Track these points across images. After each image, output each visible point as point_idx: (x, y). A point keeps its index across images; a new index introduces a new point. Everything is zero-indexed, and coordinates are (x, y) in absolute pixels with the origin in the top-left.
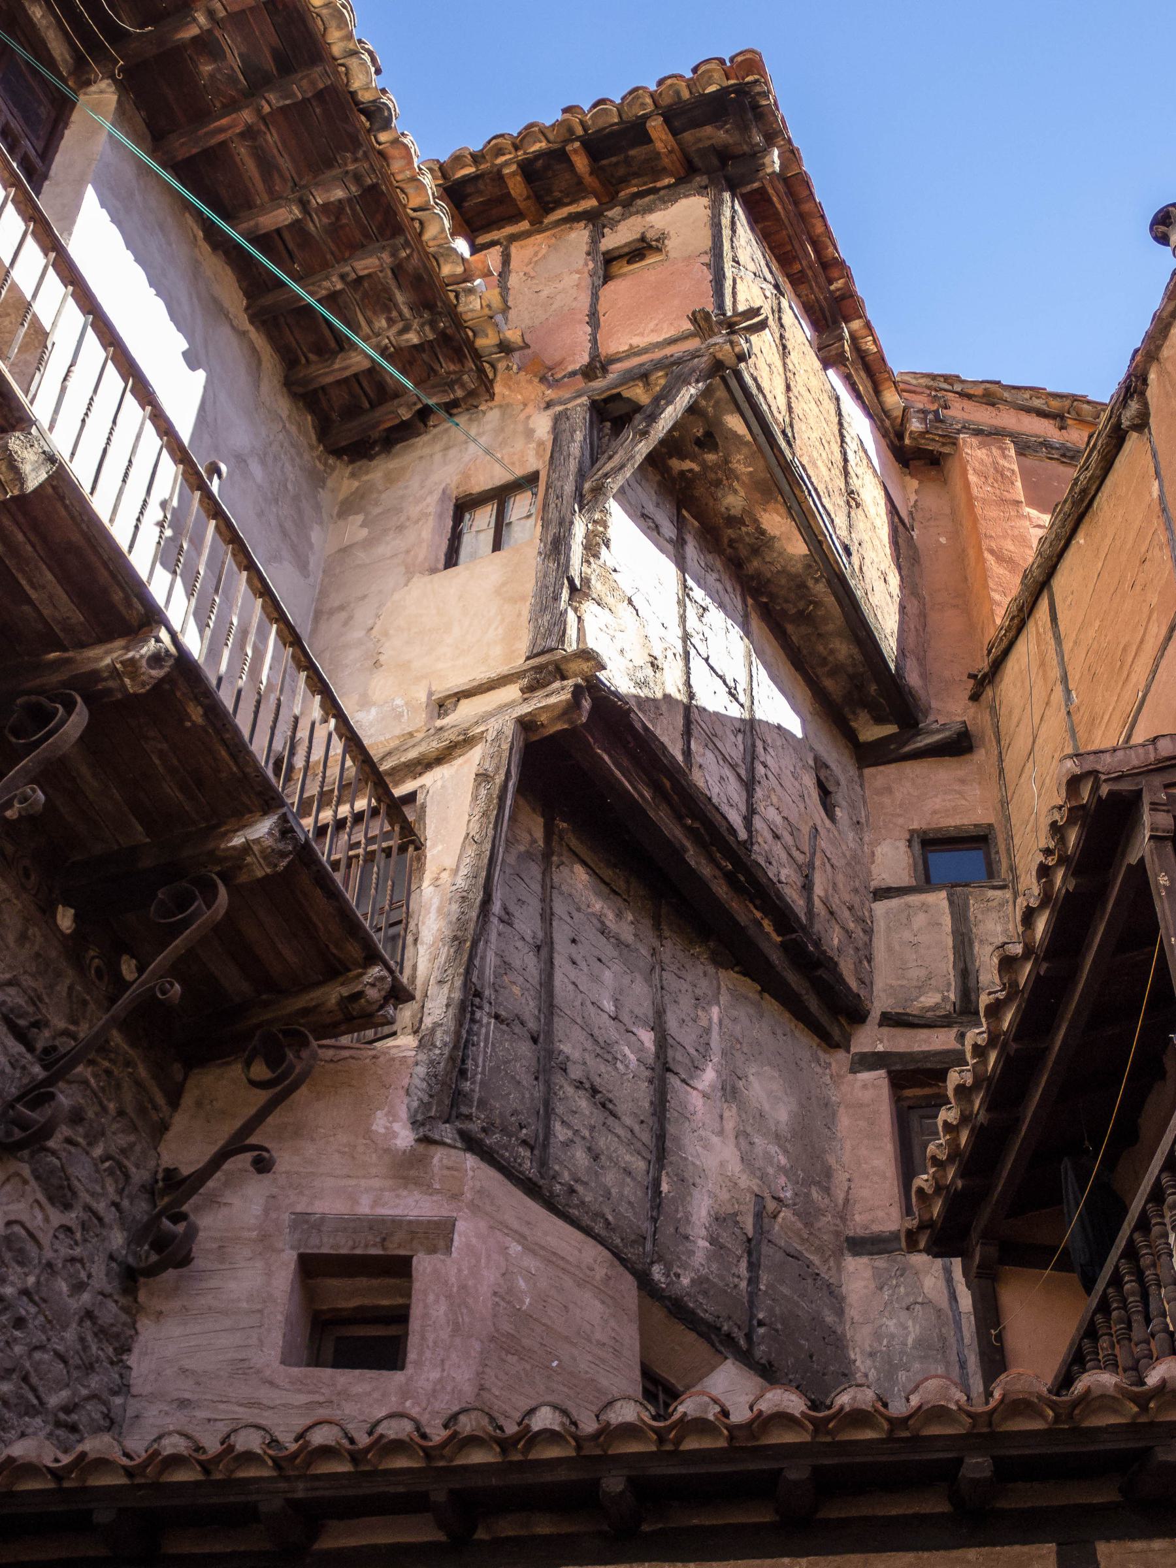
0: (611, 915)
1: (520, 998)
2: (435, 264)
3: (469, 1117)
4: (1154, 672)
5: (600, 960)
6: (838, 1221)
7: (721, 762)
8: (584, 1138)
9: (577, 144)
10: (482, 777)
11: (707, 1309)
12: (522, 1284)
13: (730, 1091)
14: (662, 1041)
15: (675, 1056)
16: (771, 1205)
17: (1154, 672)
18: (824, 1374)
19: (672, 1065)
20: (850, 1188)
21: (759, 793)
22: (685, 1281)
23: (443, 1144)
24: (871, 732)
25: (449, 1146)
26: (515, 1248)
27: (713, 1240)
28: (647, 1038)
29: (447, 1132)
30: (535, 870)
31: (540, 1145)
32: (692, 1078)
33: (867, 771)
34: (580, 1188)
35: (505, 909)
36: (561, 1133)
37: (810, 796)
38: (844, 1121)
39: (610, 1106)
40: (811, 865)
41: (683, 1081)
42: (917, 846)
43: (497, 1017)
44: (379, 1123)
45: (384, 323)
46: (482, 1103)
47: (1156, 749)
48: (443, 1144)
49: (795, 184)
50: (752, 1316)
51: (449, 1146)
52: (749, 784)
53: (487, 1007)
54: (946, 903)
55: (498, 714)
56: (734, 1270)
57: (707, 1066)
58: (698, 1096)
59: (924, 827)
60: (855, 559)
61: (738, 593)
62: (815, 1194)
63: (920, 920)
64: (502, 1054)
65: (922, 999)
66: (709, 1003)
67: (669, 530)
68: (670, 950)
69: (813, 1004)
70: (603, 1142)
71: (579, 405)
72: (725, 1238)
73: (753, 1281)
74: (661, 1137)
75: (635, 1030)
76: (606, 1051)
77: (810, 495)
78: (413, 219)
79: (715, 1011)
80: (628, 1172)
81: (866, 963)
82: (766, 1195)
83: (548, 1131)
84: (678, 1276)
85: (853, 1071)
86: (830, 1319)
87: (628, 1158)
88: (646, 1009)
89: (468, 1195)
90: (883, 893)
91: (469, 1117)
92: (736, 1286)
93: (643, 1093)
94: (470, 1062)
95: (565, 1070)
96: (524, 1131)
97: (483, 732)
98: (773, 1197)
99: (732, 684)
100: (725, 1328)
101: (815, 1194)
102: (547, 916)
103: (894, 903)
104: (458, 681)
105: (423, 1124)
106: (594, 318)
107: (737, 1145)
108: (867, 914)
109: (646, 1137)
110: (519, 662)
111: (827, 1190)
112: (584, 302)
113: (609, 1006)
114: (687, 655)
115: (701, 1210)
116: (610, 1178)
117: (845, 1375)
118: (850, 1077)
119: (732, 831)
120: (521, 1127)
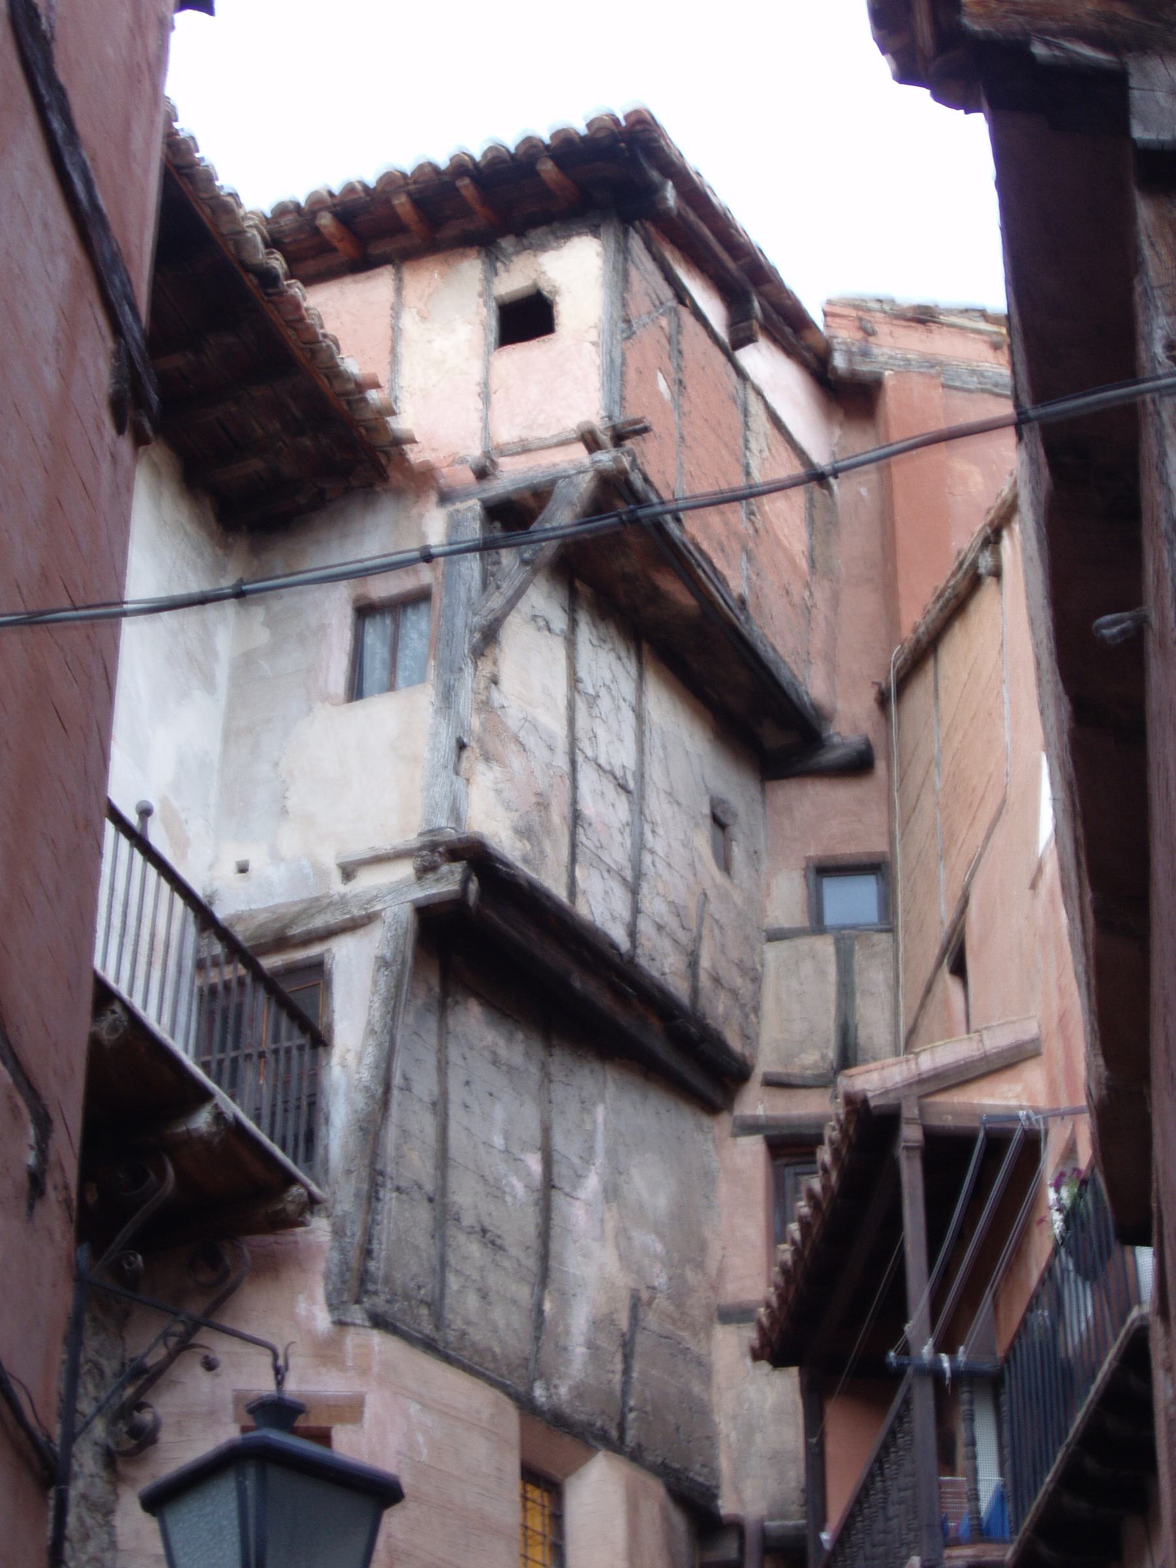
0: (501, 1042)
1: (417, 1164)
2: (326, 381)
3: (376, 1293)
4: (988, 837)
5: (491, 1094)
6: (709, 1293)
7: (606, 875)
8: (474, 1281)
9: (467, 181)
10: (383, 963)
11: (581, 1413)
12: (420, 1439)
13: (612, 1192)
14: (548, 1162)
15: (561, 1171)
16: (645, 1295)
17: (988, 837)
18: (689, 1442)
19: (556, 1182)
20: (723, 1257)
21: (645, 889)
22: (563, 1391)
23: (354, 1325)
24: (773, 738)
25: (359, 1326)
26: (414, 1408)
27: (591, 1345)
28: (534, 1163)
29: (357, 1314)
30: (432, 1023)
31: (436, 1306)
32: (575, 1188)
33: (771, 785)
34: (471, 1330)
35: (406, 1078)
36: (453, 1282)
37: (700, 858)
38: (723, 1189)
39: (498, 1241)
40: (698, 939)
41: (567, 1195)
42: (812, 876)
43: (398, 1189)
44: (302, 1307)
45: (278, 426)
46: (388, 1280)
47: (917, 1064)
48: (354, 1325)
49: (695, 195)
50: (624, 1403)
51: (359, 1326)
52: (634, 891)
53: (389, 1185)
54: (831, 950)
55: (396, 891)
56: (609, 1367)
57: (589, 1170)
58: (581, 1211)
59: (821, 853)
60: (750, 601)
61: (632, 652)
62: (690, 1275)
63: (807, 968)
64: (403, 1222)
65: (803, 1056)
66: (594, 1104)
67: (559, 621)
68: (559, 1061)
69: (697, 1080)
70: (494, 1280)
71: (469, 509)
72: (603, 1341)
73: (627, 1371)
74: (544, 1257)
75: (522, 1157)
76: (496, 1191)
77: (699, 566)
78: (302, 349)
79: (600, 1112)
80: (514, 1302)
81: (752, 1016)
82: (642, 1287)
83: (443, 1284)
84: (556, 1387)
85: (735, 1135)
86: (696, 1388)
87: (514, 1288)
88: (533, 1132)
89: (376, 1369)
90: (775, 936)
91: (376, 1293)
92: (610, 1381)
93: (530, 1221)
94: (375, 1242)
95: (458, 1220)
96: (422, 1292)
97: (382, 910)
98: (648, 1287)
99: (619, 773)
100: (599, 1424)
101: (690, 1275)
102: (442, 1068)
103: (782, 947)
104: (359, 849)
105: (338, 1309)
106: (486, 395)
107: (618, 1247)
108: (757, 959)
109: (531, 1263)
110: (411, 838)
111: (700, 1266)
112: (476, 371)
113: (498, 1141)
114: (573, 763)
115: (579, 1322)
116: (498, 1315)
117: (708, 1438)
118: (730, 1141)
119: (613, 946)
120: (419, 1288)
